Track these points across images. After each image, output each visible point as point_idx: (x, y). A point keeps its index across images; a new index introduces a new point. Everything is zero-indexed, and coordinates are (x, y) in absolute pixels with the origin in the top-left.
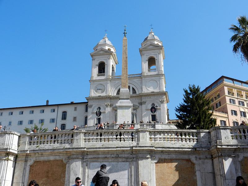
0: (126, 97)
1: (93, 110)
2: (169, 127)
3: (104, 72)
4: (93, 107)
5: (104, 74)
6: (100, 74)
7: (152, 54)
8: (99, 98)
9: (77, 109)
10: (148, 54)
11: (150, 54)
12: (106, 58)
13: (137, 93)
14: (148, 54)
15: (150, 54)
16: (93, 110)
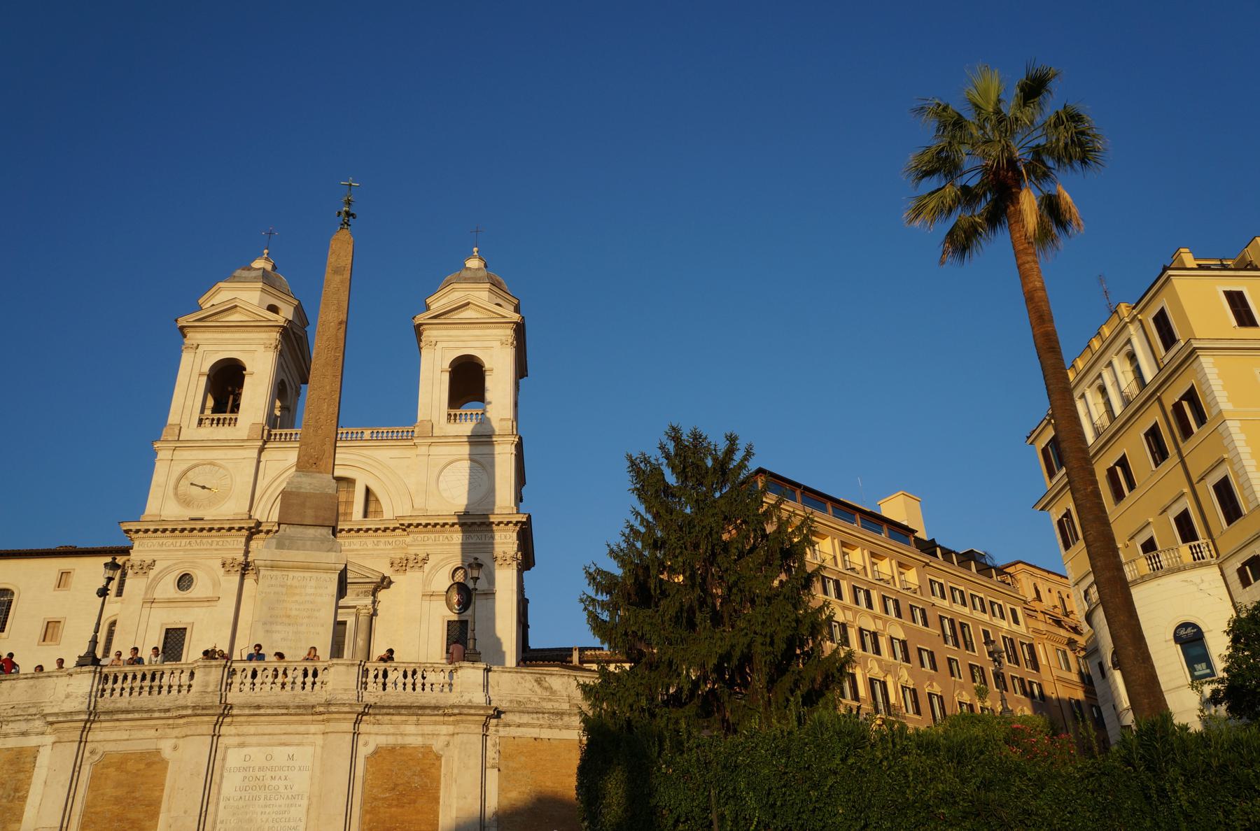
0: (317, 517)
1: (151, 587)
2: (537, 687)
3: (236, 408)
4: (152, 573)
5: (233, 416)
6: (216, 416)
7: (469, 344)
8: (192, 530)
9: (74, 580)
10: (452, 344)
11: (461, 344)
12: (253, 347)
13: (388, 513)
14: (452, 344)
15: (461, 344)
16: (151, 587)
